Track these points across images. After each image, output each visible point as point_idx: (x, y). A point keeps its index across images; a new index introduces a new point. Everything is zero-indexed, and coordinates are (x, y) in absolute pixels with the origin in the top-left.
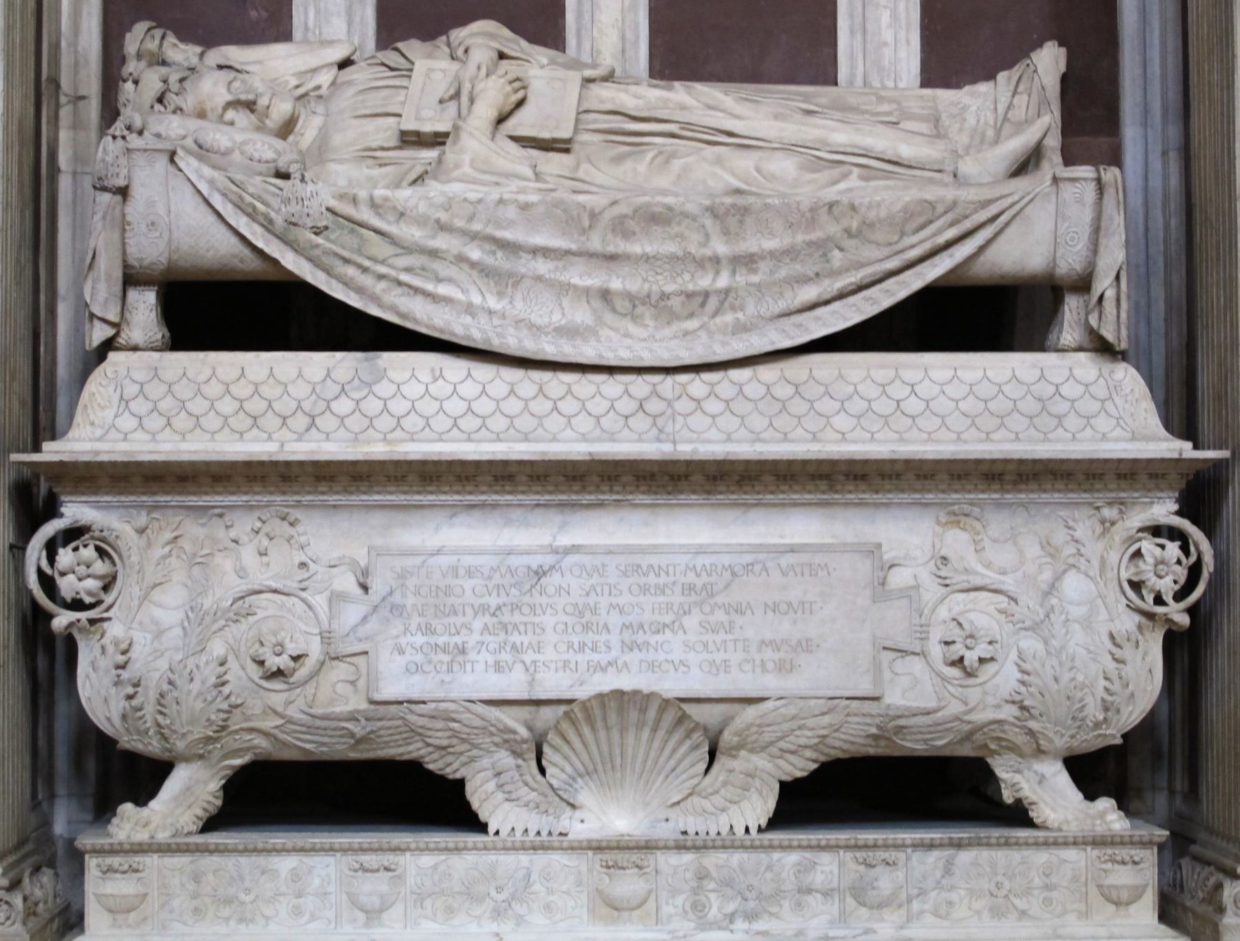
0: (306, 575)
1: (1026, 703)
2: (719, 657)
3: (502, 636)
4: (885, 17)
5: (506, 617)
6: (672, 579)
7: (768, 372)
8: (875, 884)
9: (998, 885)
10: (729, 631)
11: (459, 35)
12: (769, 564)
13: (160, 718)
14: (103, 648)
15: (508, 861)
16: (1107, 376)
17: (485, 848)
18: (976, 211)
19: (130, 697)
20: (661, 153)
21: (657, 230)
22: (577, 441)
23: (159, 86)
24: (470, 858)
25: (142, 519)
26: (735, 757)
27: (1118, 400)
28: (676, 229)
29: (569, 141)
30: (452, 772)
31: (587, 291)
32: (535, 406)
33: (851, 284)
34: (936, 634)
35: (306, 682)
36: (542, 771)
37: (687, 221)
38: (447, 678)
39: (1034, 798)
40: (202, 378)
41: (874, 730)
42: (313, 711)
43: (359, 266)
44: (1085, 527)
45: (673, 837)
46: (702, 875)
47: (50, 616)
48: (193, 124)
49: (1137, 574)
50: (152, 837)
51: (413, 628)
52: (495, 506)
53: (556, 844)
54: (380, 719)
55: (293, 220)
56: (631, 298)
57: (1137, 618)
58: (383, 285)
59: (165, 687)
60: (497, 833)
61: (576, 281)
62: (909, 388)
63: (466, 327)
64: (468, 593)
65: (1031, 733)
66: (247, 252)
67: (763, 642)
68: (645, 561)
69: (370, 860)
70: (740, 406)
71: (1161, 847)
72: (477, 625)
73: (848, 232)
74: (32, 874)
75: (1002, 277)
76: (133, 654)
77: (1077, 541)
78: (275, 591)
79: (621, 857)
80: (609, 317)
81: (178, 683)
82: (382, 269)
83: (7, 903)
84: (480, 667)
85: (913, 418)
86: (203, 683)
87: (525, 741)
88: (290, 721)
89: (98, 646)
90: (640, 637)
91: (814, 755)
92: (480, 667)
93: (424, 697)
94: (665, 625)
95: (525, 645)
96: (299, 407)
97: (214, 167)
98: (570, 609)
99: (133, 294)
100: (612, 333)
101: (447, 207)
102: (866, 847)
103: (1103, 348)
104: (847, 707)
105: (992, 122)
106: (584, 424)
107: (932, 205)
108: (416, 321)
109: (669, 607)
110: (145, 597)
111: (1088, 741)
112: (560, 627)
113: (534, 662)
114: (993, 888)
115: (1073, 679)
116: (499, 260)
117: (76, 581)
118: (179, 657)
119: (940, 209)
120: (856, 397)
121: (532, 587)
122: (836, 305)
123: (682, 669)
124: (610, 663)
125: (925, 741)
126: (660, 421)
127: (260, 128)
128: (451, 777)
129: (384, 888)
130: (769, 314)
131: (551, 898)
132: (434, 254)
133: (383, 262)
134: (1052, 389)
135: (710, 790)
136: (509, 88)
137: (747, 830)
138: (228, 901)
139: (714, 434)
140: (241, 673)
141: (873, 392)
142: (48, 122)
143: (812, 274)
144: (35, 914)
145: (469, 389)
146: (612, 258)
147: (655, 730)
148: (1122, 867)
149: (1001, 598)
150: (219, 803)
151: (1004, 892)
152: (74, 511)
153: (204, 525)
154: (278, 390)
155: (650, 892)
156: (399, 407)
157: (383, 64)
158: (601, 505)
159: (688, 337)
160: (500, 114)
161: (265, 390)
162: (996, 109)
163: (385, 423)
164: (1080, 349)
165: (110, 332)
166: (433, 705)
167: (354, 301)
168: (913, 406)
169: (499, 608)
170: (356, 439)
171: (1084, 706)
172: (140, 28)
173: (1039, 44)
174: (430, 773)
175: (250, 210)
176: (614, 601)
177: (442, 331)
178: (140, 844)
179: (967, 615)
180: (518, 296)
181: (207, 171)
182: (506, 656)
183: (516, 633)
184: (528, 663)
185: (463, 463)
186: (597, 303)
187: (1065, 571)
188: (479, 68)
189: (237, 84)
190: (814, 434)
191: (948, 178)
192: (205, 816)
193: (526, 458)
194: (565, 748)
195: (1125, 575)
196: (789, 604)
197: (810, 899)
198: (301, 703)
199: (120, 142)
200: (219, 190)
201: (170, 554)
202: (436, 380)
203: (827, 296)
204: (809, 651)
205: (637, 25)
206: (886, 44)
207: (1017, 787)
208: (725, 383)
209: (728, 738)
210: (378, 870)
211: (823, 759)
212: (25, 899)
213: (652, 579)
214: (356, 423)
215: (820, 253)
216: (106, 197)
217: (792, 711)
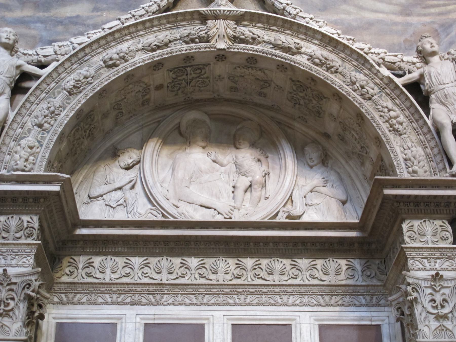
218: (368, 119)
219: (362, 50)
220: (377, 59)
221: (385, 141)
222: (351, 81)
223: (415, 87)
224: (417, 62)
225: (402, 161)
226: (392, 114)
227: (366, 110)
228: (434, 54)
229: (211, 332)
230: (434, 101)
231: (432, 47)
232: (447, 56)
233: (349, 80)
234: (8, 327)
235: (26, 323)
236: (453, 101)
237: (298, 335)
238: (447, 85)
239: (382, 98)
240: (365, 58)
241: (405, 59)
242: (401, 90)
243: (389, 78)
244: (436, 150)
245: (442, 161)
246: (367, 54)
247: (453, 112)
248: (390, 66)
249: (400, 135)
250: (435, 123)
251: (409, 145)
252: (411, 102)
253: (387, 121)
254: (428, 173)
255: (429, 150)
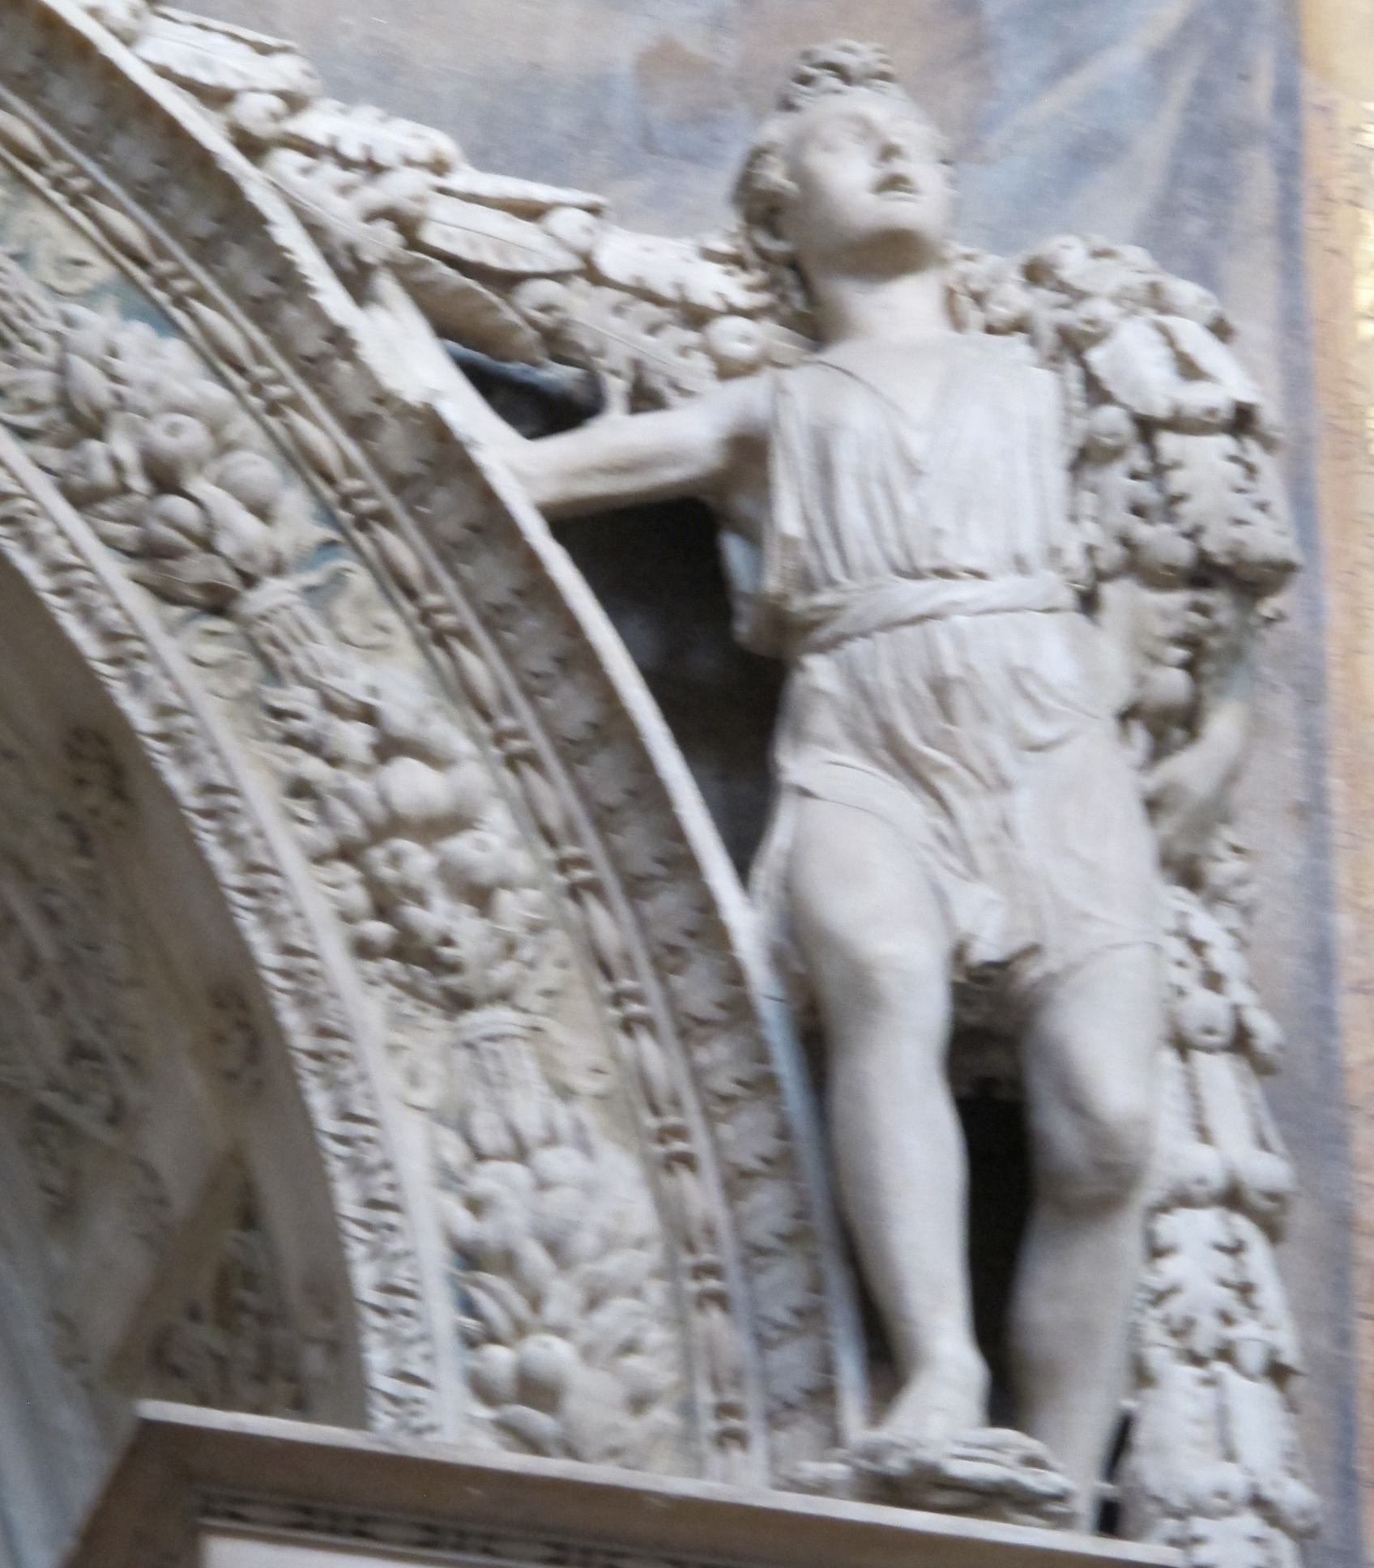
218: (168, 797)
219: (216, 98)
220: (343, 215)
221: (302, 1040)
222: (64, 400)
223: (668, 553)
224: (733, 311)
225: (432, 1263)
226: (412, 784)
227: (164, 711)
228: (893, 253)
230: (824, 722)
231: (894, 183)
232: (1015, 298)
233: (41, 384)
236: (1001, 748)
238: (964, 591)
239: (342, 608)
240: (231, 189)
241: (622, 253)
242: (532, 561)
243: (433, 428)
244: (769, 1206)
245: (810, 1317)
246: (252, 147)
247: (984, 857)
248: (472, 316)
249: (459, 1003)
250: (800, 941)
251: (531, 1109)
252: (609, 696)
253: (348, 852)
254: (662, 1415)
255: (701, 1195)
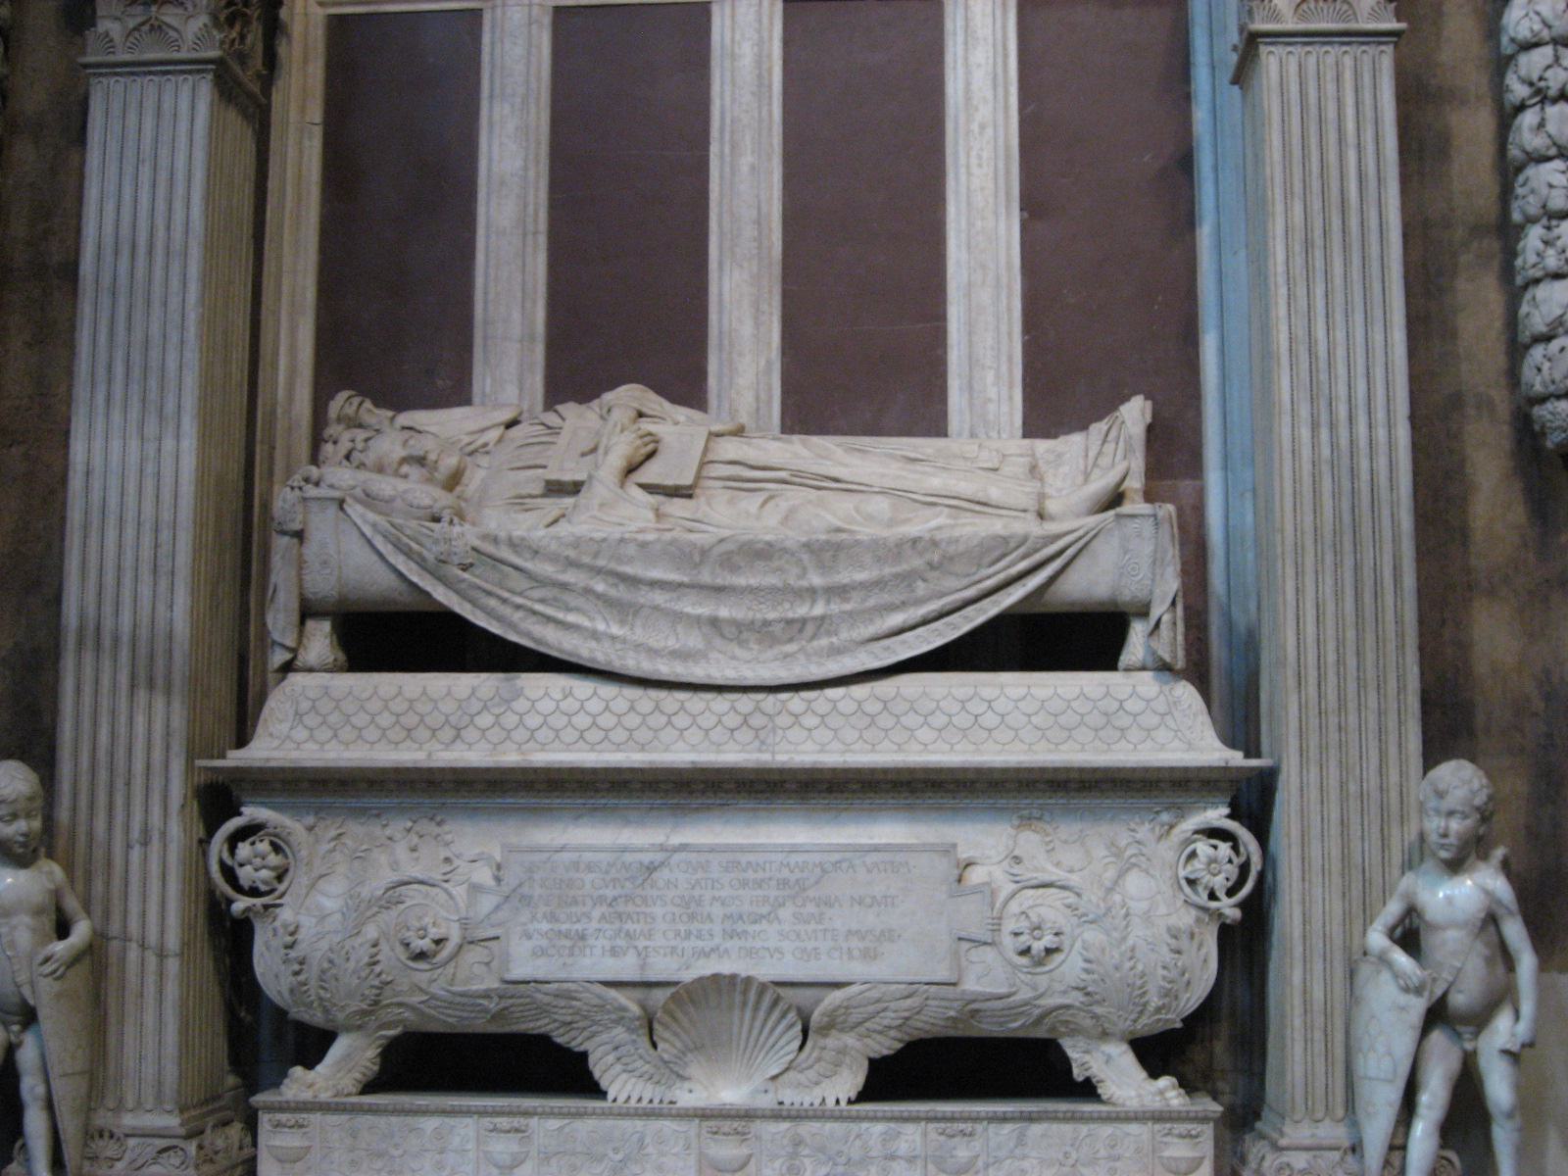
0: (448, 869)
1: (1090, 989)
2: (810, 945)
3: (617, 925)
4: (990, 376)
5: (621, 908)
6: (768, 875)
7: (859, 691)
8: (954, 1153)
9: (1066, 1155)
10: (820, 922)
11: (608, 397)
12: (857, 862)
13: (322, 992)
14: (275, 931)
15: (626, 1124)
16: (1167, 693)
17: (603, 1114)
18: (1045, 545)
19: (297, 973)
20: (771, 498)
21: (760, 564)
22: (689, 751)
23: (349, 445)
24: (590, 1123)
25: (310, 820)
26: (825, 1036)
27: (1176, 714)
28: (776, 564)
29: (690, 487)
30: (578, 1045)
31: (698, 620)
32: (653, 721)
33: (933, 611)
34: (1010, 925)
35: (447, 963)
36: (654, 1045)
37: (787, 556)
38: (570, 961)
39: (1102, 1076)
40: (366, 695)
41: (952, 1013)
42: (454, 989)
43: (499, 597)
44: (1144, 831)
45: (770, 1107)
46: (798, 1142)
47: (230, 902)
48: (363, 475)
49: (1192, 872)
50: (316, 1097)
51: (539, 916)
52: (615, 809)
53: (665, 1111)
54: (512, 997)
55: (442, 557)
56: (739, 626)
57: (1194, 912)
58: (517, 616)
59: (326, 965)
60: (615, 1100)
61: (689, 609)
62: (986, 704)
63: (591, 650)
64: (588, 886)
65: (1095, 1017)
66: (403, 587)
67: (849, 931)
68: (744, 858)
69: (503, 1122)
70: (835, 721)
71: (1217, 1122)
72: (596, 913)
73: (931, 566)
74: (215, 1127)
75: (1073, 604)
76: (300, 936)
77: (1138, 842)
78: (422, 882)
79: (727, 1125)
80: (718, 642)
81: (336, 961)
82: (519, 600)
83: (182, 1149)
84: (598, 951)
85: (990, 730)
86: (358, 962)
87: (638, 1019)
88: (433, 997)
89: (270, 927)
90: (740, 927)
91: (899, 1035)
92: (598, 951)
93: (550, 977)
94: (763, 917)
95: (638, 932)
96: (447, 721)
97: (380, 513)
98: (678, 901)
99: (310, 624)
100: (721, 656)
101: (577, 543)
102: (944, 1119)
103: (1164, 668)
104: (926, 991)
105: (1082, 467)
106: (694, 736)
107: (1005, 540)
108: (547, 645)
109: (766, 899)
110: (312, 886)
111: (1146, 1025)
112: (669, 917)
113: (646, 948)
114: (1061, 1156)
115: (1132, 969)
116: (621, 592)
117: (252, 871)
118: (337, 938)
119: (1012, 545)
120: (938, 713)
121: (644, 881)
122: (920, 630)
123: (777, 955)
124: (712, 950)
125: (1001, 1024)
126: (762, 734)
127: (430, 480)
128: (576, 1049)
129: (515, 1148)
130: (859, 639)
131: (664, 1159)
132: (564, 586)
133: (520, 594)
134: (1116, 705)
135: (804, 1066)
136: (639, 442)
137: (838, 1102)
138: (380, 1155)
139: (809, 746)
140: (391, 954)
141: (955, 708)
142: (261, 479)
143: (897, 602)
144: (212, 1161)
145: (594, 706)
146: (719, 590)
147: (756, 1009)
148: (1181, 1141)
149: (1067, 893)
150: (376, 1068)
151: (1071, 1161)
152: (252, 813)
153: (363, 824)
154: (428, 707)
155: (750, 1156)
156: (533, 721)
157: (543, 424)
158: (708, 808)
159: (788, 659)
160: (630, 463)
161: (420, 707)
162: (1087, 456)
163: (520, 735)
164: (1143, 668)
165: (288, 656)
166: (556, 985)
167: (495, 628)
168: (990, 720)
169: (615, 899)
170: (494, 749)
171: (1144, 993)
172: (343, 395)
173: (1126, 399)
174: (559, 1048)
175: (406, 549)
176: (717, 894)
177: (570, 654)
178: (304, 1103)
179: (1036, 909)
180: (638, 623)
181: (371, 516)
182: (621, 942)
183: (629, 921)
184: (640, 947)
185: (582, 771)
186: (706, 629)
187: (1128, 869)
188: (615, 426)
189: (412, 442)
190: (899, 745)
191: (1031, 516)
192: (365, 1080)
193: (636, 766)
194: (674, 1026)
195: (1182, 873)
196: (874, 897)
197: (894, 1164)
198: (442, 982)
199: (297, 492)
200: (380, 533)
201: (334, 850)
202: (566, 697)
203: (911, 622)
204: (891, 940)
205: (770, 389)
206: (990, 400)
207: (1086, 1066)
208: (822, 699)
209: (816, 1018)
210: (509, 1132)
211: (907, 1038)
212: (200, 1147)
213: (750, 875)
214: (495, 735)
215: (906, 583)
216: (286, 540)
217: (875, 994)
229: (728, 22)
234: (176, 30)
235: (222, 18)
237: (960, 23)
